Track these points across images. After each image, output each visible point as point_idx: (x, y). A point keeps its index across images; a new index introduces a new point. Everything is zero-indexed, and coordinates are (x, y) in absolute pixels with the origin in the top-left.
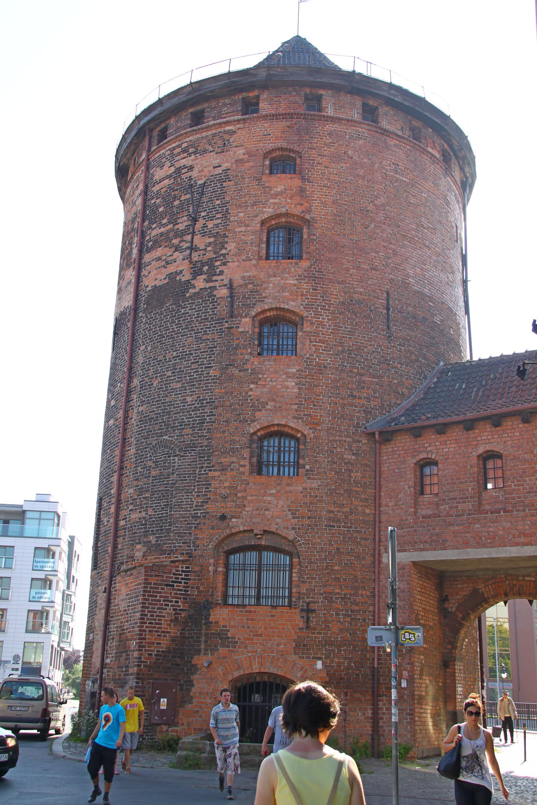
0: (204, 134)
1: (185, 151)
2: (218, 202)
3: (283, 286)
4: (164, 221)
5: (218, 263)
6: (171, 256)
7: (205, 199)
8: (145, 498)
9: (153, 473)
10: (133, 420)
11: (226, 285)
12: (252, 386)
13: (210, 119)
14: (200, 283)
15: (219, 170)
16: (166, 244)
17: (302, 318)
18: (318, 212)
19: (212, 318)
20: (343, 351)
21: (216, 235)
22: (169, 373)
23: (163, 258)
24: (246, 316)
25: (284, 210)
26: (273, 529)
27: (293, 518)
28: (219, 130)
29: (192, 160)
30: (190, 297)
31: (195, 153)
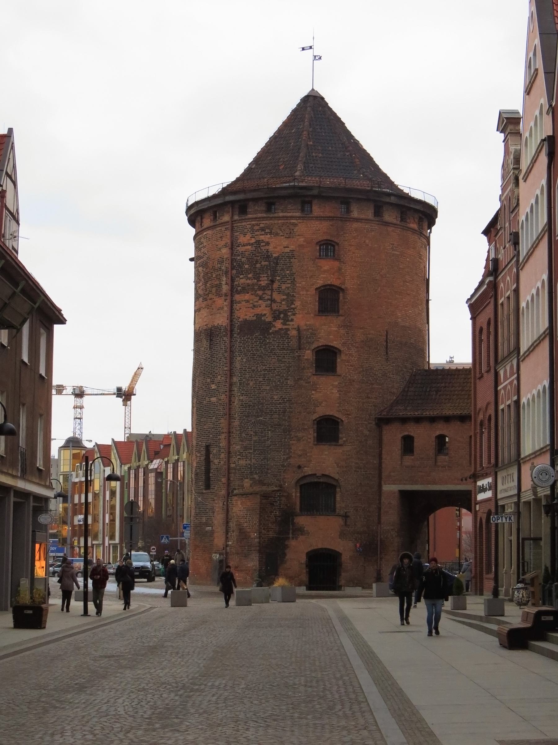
0: (276, 222)
1: (263, 229)
2: (288, 272)
3: (329, 331)
4: (250, 276)
5: (289, 314)
6: (256, 302)
7: (279, 268)
8: (249, 453)
9: (254, 438)
10: (235, 404)
11: (295, 329)
12: (313, 392)
13: (279, 211)
14: (278, 325)
15: (287, 250)
16: (253, 293)
17: (340, 351)
18: (349, 284)
19: (288, 349)
20: (363, 371)
21: (288, 295)
22: (261, 379)
23: (251, 302)
24: (308, 349)
25: (329, 282)
26: (327, 473)
27: (338, 467)
28: (286, 221)
29: (269, 238)
30: (272, 333)
31: (271, 233)
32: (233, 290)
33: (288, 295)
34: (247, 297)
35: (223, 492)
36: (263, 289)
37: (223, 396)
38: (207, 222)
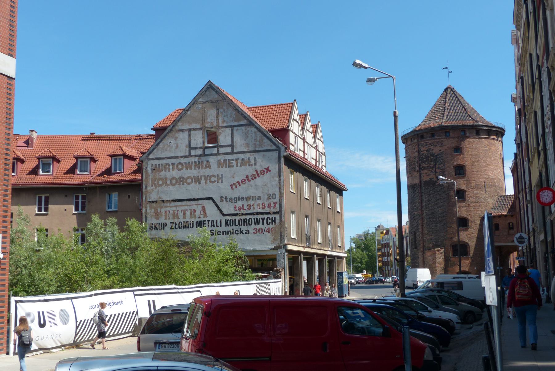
1: (430, 144)
21: (442, 169)
32: (420, 169)
33: (442, 169)
34: (426, 171)
35: (422, 249)
36: (432, 168)
37: (419, 212)
38: (409, 143)
